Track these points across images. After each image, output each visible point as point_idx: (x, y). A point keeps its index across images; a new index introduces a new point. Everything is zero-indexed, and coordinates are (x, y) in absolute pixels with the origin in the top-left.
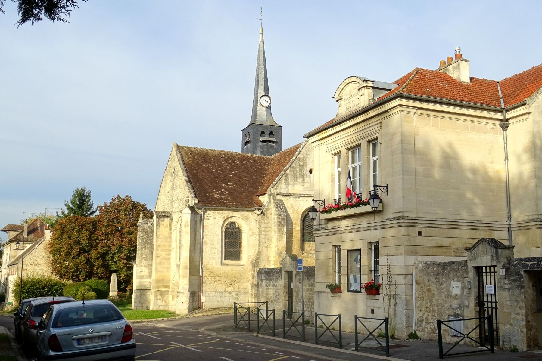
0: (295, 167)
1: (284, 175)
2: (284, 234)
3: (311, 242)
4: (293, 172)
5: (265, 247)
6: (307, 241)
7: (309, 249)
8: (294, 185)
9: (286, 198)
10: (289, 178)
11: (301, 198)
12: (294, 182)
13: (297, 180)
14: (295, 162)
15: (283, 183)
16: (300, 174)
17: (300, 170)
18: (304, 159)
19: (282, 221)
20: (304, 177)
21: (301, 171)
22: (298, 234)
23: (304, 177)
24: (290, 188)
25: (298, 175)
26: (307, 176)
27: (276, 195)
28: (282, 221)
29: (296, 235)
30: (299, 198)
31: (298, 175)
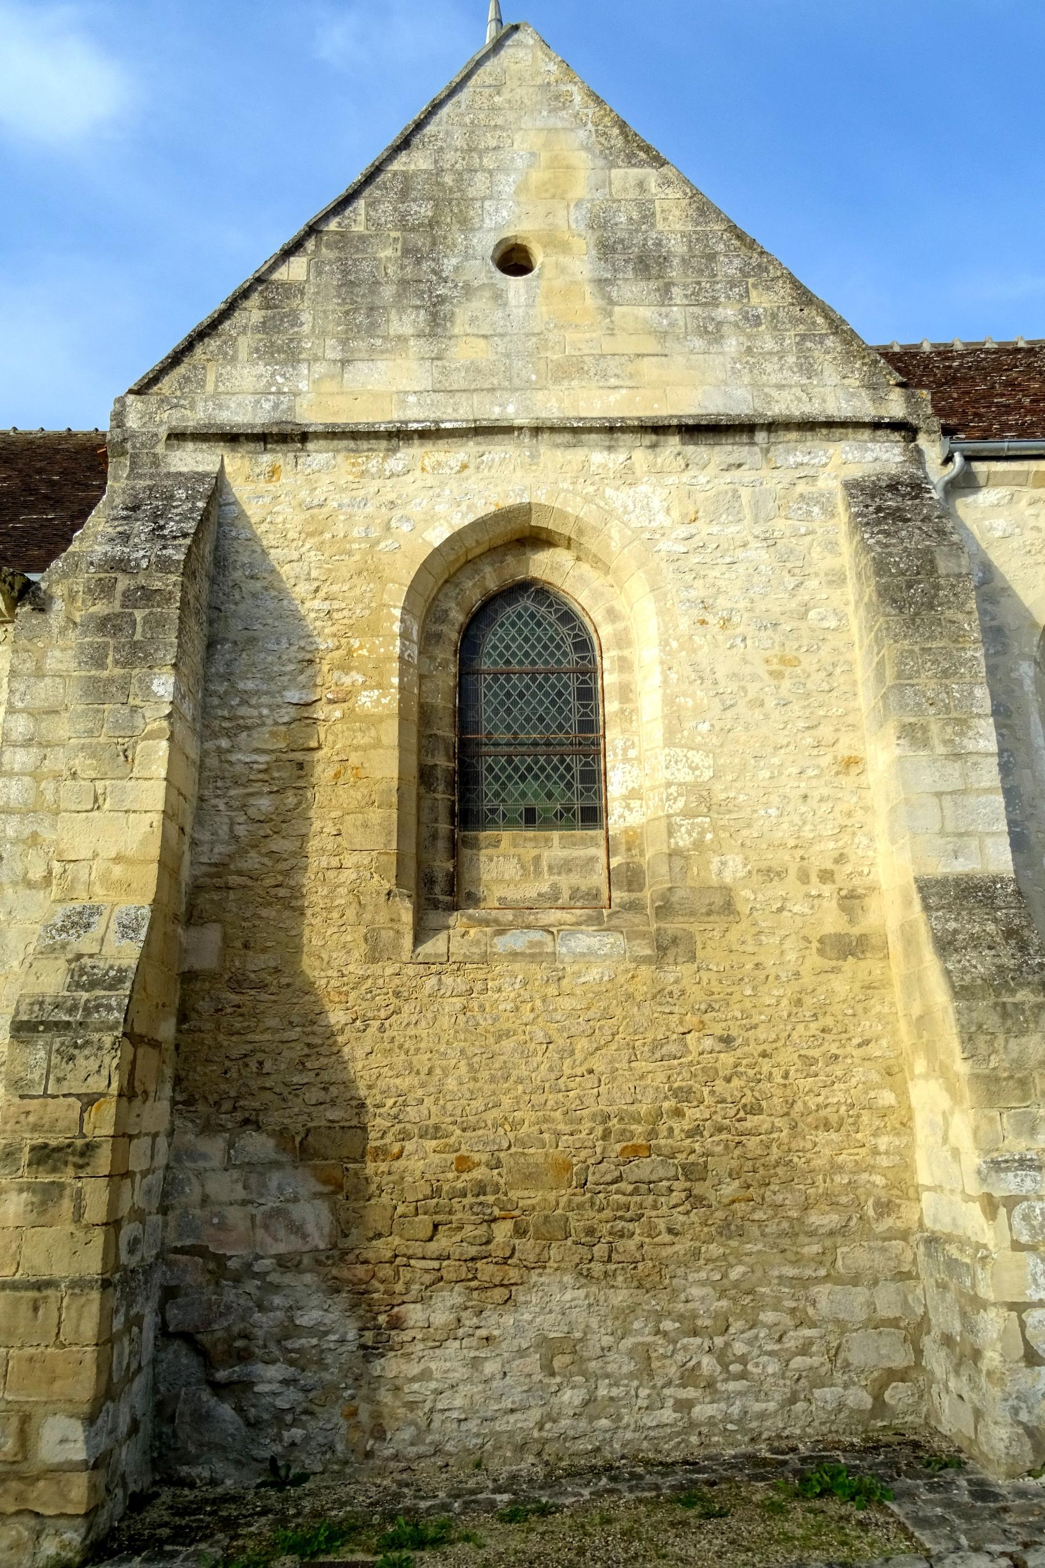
0: (362, 238)
1: (255, 299)
2: (151, 736)
3: (548, 824)
4: (346, 273)
5: (30, 885)
6: (510, 823)
7: (531, 890)
8: (345, 362)
9: (266, 458)
10: (306, 317)
11: (409, 454)
12: (344, 342)
13: (373, 325)
14: (361, 204)
15: (243, 353)
16: (403, 283)
17: (406, 252)
18: (448, 179)
19: (139, 615)
20: (442, 300)
21: (418, 262)
22: (377, 744)
23: (442, 300)
24: (303, 386)
25: (388, 292)
26: (468, 290)
27: (168, 447)
28: (139, 615)
29: (354, 759)
30: (395, 450)
31: (388, 292)
